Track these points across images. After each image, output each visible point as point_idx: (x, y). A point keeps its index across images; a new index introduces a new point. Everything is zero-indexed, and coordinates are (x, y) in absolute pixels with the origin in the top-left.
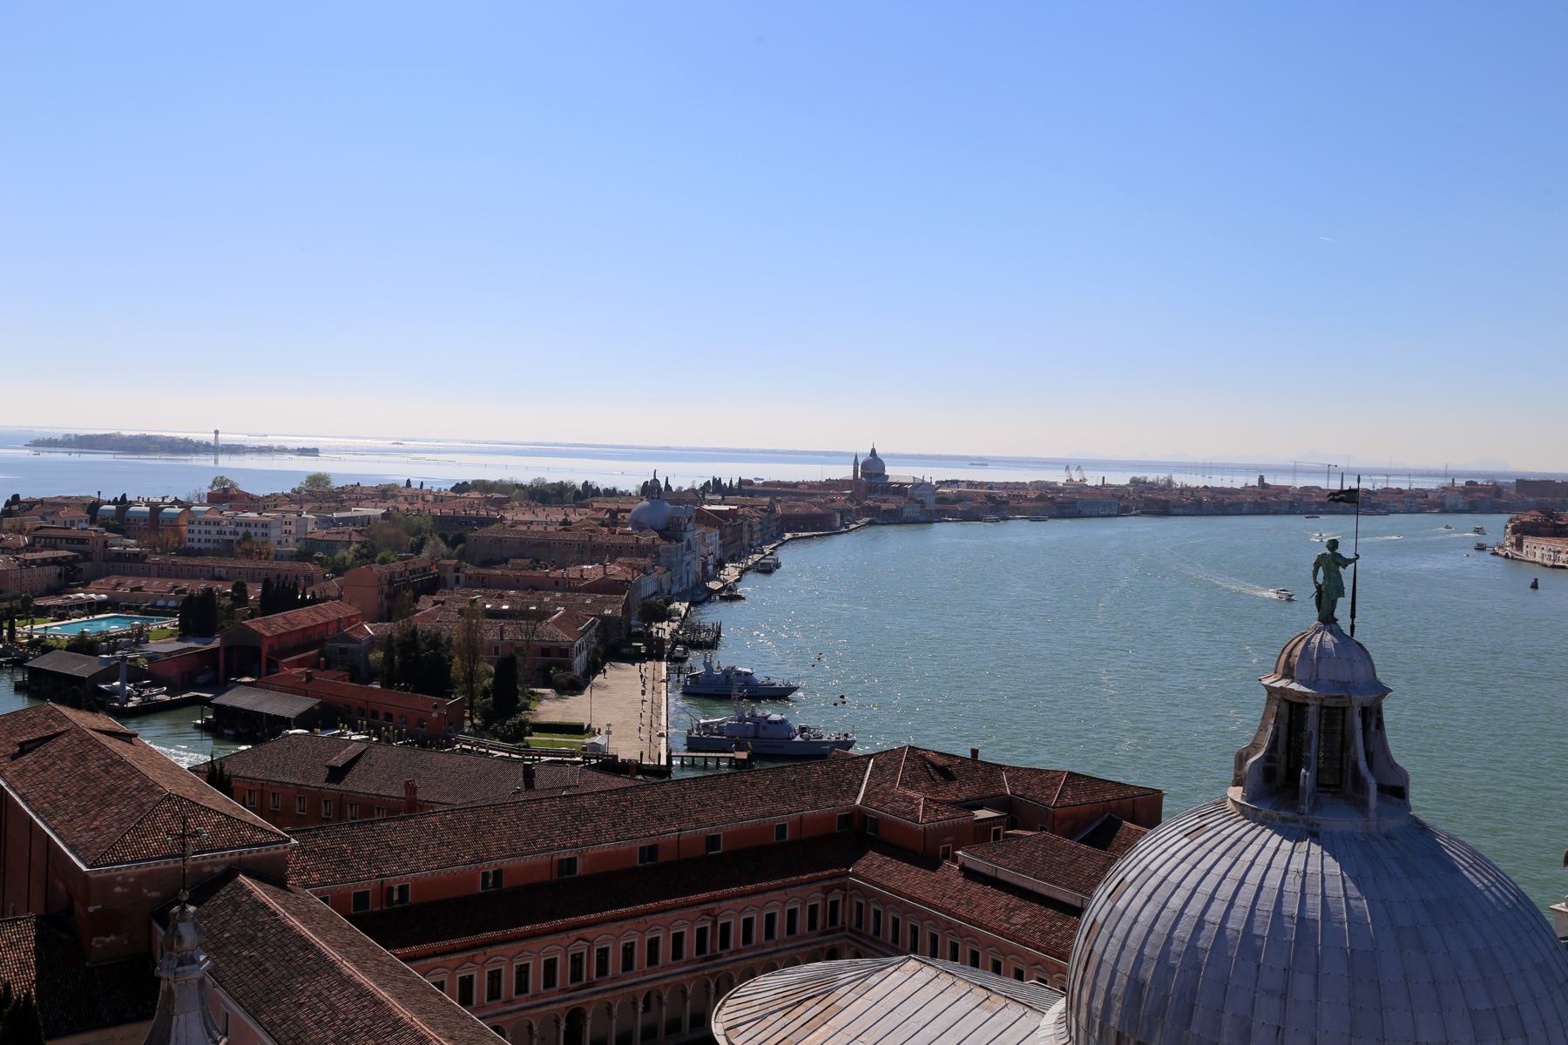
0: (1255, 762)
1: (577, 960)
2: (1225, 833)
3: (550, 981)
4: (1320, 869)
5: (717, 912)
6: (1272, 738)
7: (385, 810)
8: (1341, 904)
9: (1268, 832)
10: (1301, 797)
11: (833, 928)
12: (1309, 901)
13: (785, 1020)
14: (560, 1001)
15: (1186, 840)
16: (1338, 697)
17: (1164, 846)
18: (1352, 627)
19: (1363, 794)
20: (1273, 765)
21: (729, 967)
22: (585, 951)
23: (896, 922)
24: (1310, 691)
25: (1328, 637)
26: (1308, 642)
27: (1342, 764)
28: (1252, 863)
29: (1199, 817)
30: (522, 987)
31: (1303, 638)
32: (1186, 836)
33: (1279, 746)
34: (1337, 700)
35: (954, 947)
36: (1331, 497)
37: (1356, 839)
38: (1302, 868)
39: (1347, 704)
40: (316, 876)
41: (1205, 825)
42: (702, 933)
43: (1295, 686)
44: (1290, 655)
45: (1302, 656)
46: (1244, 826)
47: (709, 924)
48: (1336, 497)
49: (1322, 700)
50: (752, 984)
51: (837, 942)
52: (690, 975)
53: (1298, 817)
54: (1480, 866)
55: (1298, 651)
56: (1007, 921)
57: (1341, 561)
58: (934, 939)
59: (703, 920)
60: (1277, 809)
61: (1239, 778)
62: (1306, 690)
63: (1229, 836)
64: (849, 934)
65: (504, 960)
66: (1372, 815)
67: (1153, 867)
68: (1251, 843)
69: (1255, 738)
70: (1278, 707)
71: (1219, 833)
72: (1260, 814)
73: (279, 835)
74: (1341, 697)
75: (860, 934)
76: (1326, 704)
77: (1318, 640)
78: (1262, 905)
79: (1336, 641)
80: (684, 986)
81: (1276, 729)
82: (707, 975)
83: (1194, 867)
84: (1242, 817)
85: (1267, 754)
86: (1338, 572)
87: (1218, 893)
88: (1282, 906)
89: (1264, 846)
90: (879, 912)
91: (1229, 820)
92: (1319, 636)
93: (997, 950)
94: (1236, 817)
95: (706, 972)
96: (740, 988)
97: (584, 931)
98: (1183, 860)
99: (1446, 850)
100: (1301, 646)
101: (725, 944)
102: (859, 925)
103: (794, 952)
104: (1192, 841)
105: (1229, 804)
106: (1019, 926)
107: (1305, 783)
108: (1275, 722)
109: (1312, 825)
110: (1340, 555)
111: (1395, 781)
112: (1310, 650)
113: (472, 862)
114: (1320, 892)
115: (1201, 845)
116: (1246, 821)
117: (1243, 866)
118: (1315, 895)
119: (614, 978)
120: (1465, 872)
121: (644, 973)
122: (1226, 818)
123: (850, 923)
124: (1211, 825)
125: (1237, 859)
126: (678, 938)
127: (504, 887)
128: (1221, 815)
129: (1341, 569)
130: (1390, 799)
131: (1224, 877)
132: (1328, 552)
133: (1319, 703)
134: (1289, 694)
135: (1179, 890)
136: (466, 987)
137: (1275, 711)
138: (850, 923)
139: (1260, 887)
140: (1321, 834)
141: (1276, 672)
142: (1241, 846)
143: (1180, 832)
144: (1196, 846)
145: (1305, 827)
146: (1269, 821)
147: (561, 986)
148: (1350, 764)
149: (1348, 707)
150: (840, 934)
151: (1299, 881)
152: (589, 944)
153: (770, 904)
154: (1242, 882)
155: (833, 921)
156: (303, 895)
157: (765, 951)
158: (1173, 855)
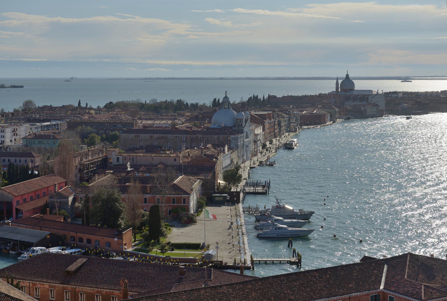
7: (101, 296)
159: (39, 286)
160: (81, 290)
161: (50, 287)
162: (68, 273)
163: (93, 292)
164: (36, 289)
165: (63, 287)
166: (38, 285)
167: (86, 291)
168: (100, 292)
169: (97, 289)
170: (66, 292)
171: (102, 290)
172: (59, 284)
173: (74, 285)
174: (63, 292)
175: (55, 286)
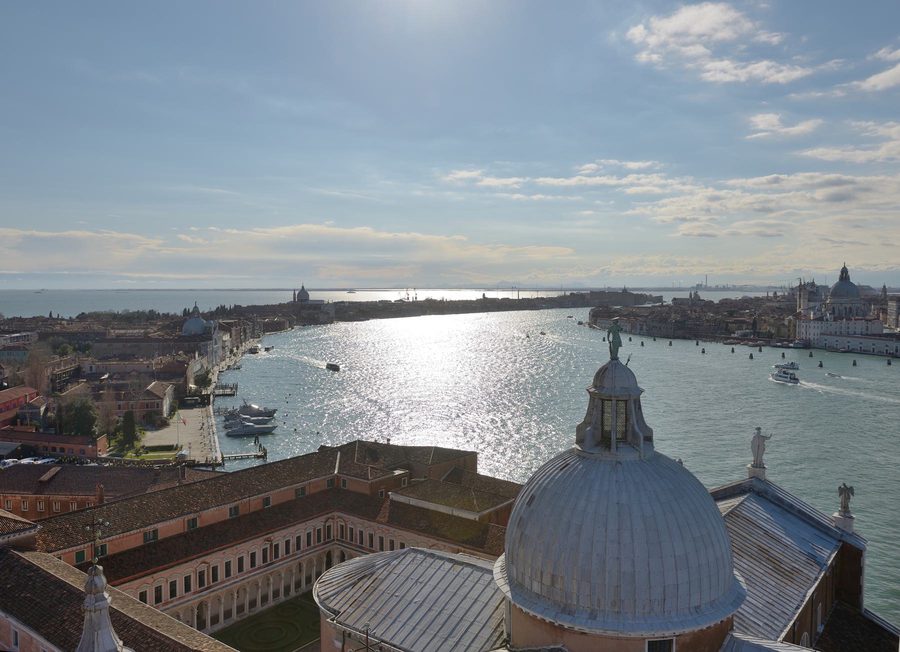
1: (201, 574)
3: (188, 588)
5: (272, 538)
7: (76, 503)
11: (329, 540)
13: (354, 590)
14: (195, 599)
21: (280, 568)
22: (206, 569)
23: (361, 533)
30: (173, 593)
35: (392, 543)
40: (53, 545)
42: (265, 551)
47: (268, 546)
50: (327, 574)
51: (331, 547)
52: (260, 575)
56: (418, 526)
58: (381, 539)
59: (266, 544)
64: (336, 542)
65: (162, 578)
73: (30, 524)
75: (343, 542)
80: (257, 581)
82: (269, 573)
90: (352, 529)
93: (413, 541)
95: (268, 572)
96: (322, 577)
97: (204, 558)
101: (276, 556)
102: (342, 537)
103: (311, 555)
106: (423, 528)
113: (141, 527)
119: (222, 582)
121: (237, 577)
123: (337, 536)
126: (253, 556)
127: (159, 539)
136: (143, 597)
138: (337, 536)
147: (194, 590)
150: (332, 543)
152: (208, 565)
153: (298, 532)
155: (329, 537)
156: (48, 557)
157: (297, 557)
159: (10, 498)
160: (56, 499)
161: (22, 499)
162: (41, 482)
163: (68, 499)
164: (7, 501)
165: (36, 497)
166: (9, 498)
167: (60, 499)
168: (75, 499)
169: (71, 497)
170: (39, 502)
171: (77, 497)
172: (33, 494)
173: (47, 495)
174: (36, 504)
175: (28, 497)
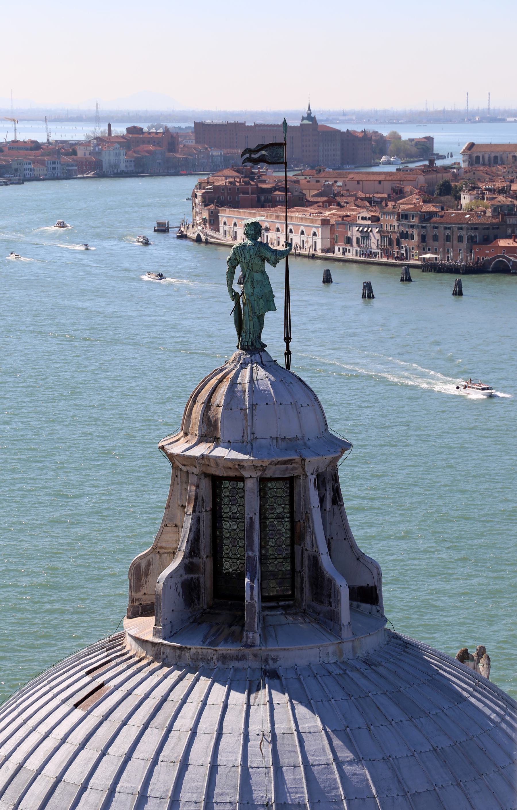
0: (171, 576)
2: (141, 691)
4: (293, 725)
6: (192, 536)
8: (333, 773)
9: (204, 682)
10: (247, 620)
12: (288, 776)
15: (79, 713)
16: (285, 462)
17: (43, 729)
18: (288, 353)
19: (330, 604)
20: (197, 576)
24: (241, 456)
25: (261, 373)
26: (234, 383)
27: (293, 563)
28: (194, 732)
29: (88, 673)
31: (224, 377)
32: (76, 706)
33: (202, 546)
34: (284, 467)
36: (248, 155)
37: (330, 673)
38: (268, 728)
39: (296, 473)
41: (102, 685)
43: (221, 452)
44: (208, 405)
45: (228, 405)
46: (165, 677)
48: (254, 156)
49: (264, 469)
53: (246, 651)
54: (484, 689)
55: (220, 398)
57: (269, 255)
60: (212, 643)
61: (137, 604)
62: (241, 456)
63: (147, 696)
66: (346, 634)
67: (33, 764)
68: (184, 701)
69: (158, 539)
70: (197, 486)
71: (129, 693)
72: (187, 655)
74: (290, 461)
76: (268, 474)
77: (247, 379)
78: (222, 794)
79: (273, 379)
81: (197, 521)
83: (104, 753)
84: (156, 664)
85: (187, 561)
86: (264, 273)
87: (150, 788)
88: (251, 792)
89: (204, 703)
91: (139, 670)
92: (247, 372)
94: (149, 664)
98: (83, 745)
99: (441, 671)
100: (224, 388)
104: (89, 713)
105: (129, 644)
107: (252, 598)
108: (194, 511)
109: (266, 661)
110: (266, 246)
111: (364, 581)
112: (239, 394)
114: (300, 760)
115: (106, 717)
116: (165, 670)
117: (179, 739)
118: (295, 767)
120: (473, 700)
122: (134, 668)
124: (112, 684)
125: (169, 730)
128: (123, 666)
129: (268, 267)
130: (358, 606)
131: (155, 762)
132: (248, 242)
133: (259, 473)
134: (212, 464)
135: (85, 794)
137: (193, 493)
139: (214, 768)
140: (281, 672)
141: (186, 434)
142: (169, 709)
143: (64, 701)
144: (98, 720)
145: (256, 665)
146: (201, 664)
148: (306, 562)
149: (298, 477)
151: (268, 749)
154: (184, 765)
158: (64, 741)
